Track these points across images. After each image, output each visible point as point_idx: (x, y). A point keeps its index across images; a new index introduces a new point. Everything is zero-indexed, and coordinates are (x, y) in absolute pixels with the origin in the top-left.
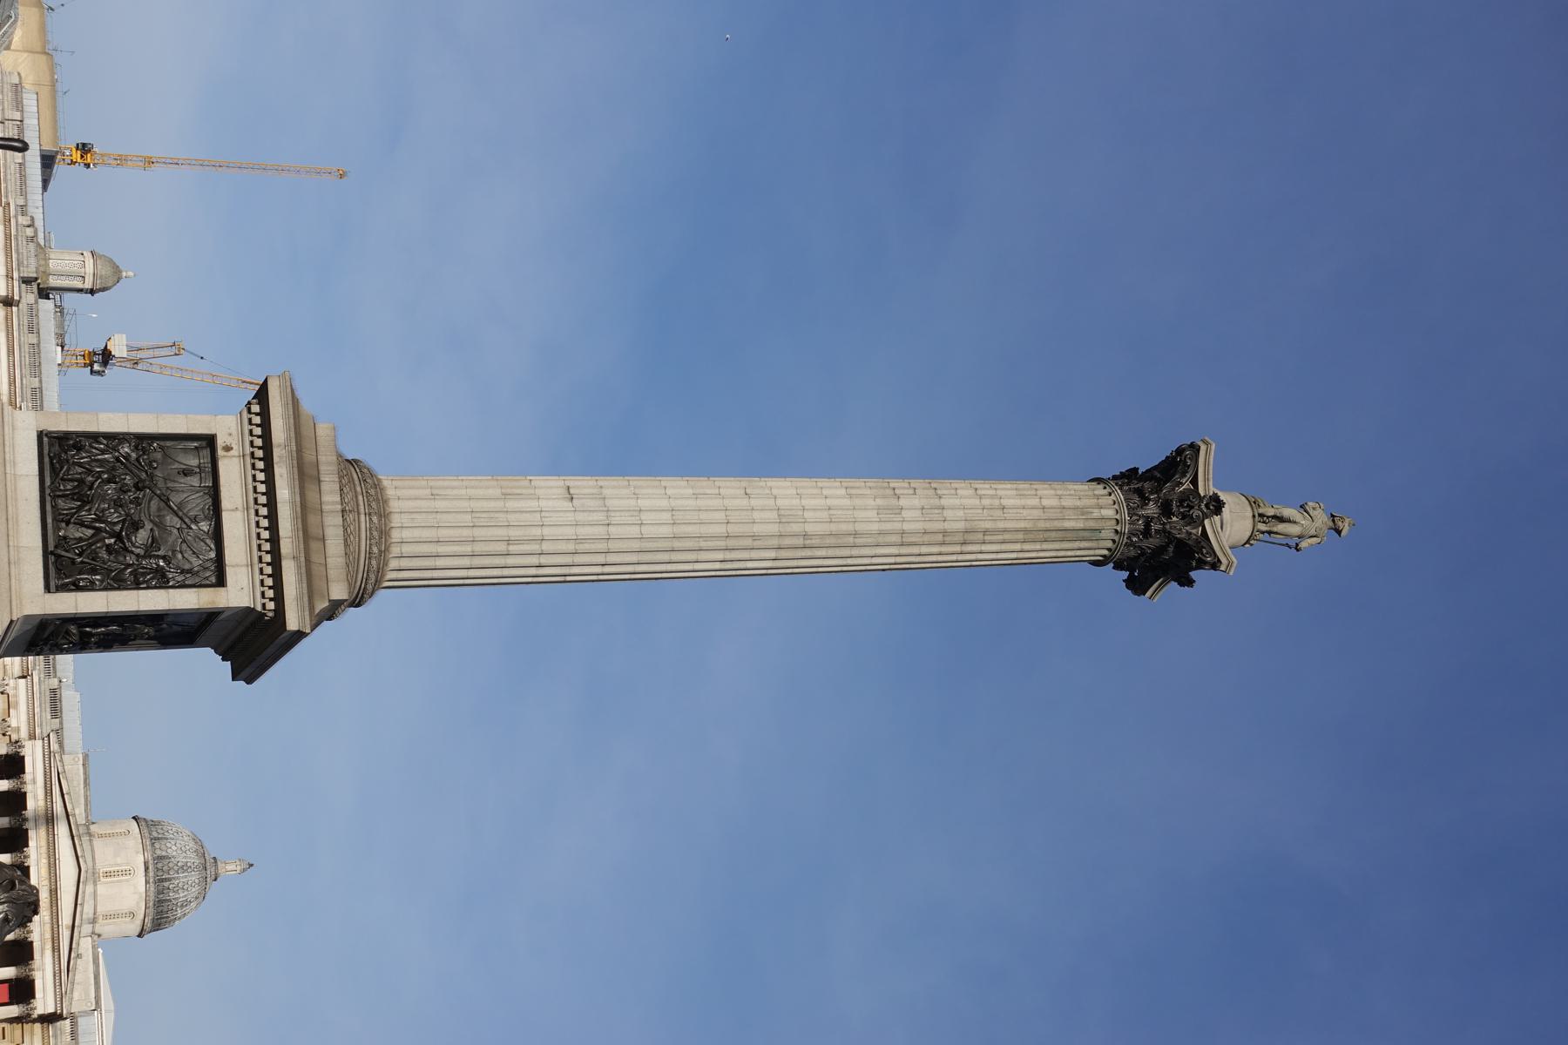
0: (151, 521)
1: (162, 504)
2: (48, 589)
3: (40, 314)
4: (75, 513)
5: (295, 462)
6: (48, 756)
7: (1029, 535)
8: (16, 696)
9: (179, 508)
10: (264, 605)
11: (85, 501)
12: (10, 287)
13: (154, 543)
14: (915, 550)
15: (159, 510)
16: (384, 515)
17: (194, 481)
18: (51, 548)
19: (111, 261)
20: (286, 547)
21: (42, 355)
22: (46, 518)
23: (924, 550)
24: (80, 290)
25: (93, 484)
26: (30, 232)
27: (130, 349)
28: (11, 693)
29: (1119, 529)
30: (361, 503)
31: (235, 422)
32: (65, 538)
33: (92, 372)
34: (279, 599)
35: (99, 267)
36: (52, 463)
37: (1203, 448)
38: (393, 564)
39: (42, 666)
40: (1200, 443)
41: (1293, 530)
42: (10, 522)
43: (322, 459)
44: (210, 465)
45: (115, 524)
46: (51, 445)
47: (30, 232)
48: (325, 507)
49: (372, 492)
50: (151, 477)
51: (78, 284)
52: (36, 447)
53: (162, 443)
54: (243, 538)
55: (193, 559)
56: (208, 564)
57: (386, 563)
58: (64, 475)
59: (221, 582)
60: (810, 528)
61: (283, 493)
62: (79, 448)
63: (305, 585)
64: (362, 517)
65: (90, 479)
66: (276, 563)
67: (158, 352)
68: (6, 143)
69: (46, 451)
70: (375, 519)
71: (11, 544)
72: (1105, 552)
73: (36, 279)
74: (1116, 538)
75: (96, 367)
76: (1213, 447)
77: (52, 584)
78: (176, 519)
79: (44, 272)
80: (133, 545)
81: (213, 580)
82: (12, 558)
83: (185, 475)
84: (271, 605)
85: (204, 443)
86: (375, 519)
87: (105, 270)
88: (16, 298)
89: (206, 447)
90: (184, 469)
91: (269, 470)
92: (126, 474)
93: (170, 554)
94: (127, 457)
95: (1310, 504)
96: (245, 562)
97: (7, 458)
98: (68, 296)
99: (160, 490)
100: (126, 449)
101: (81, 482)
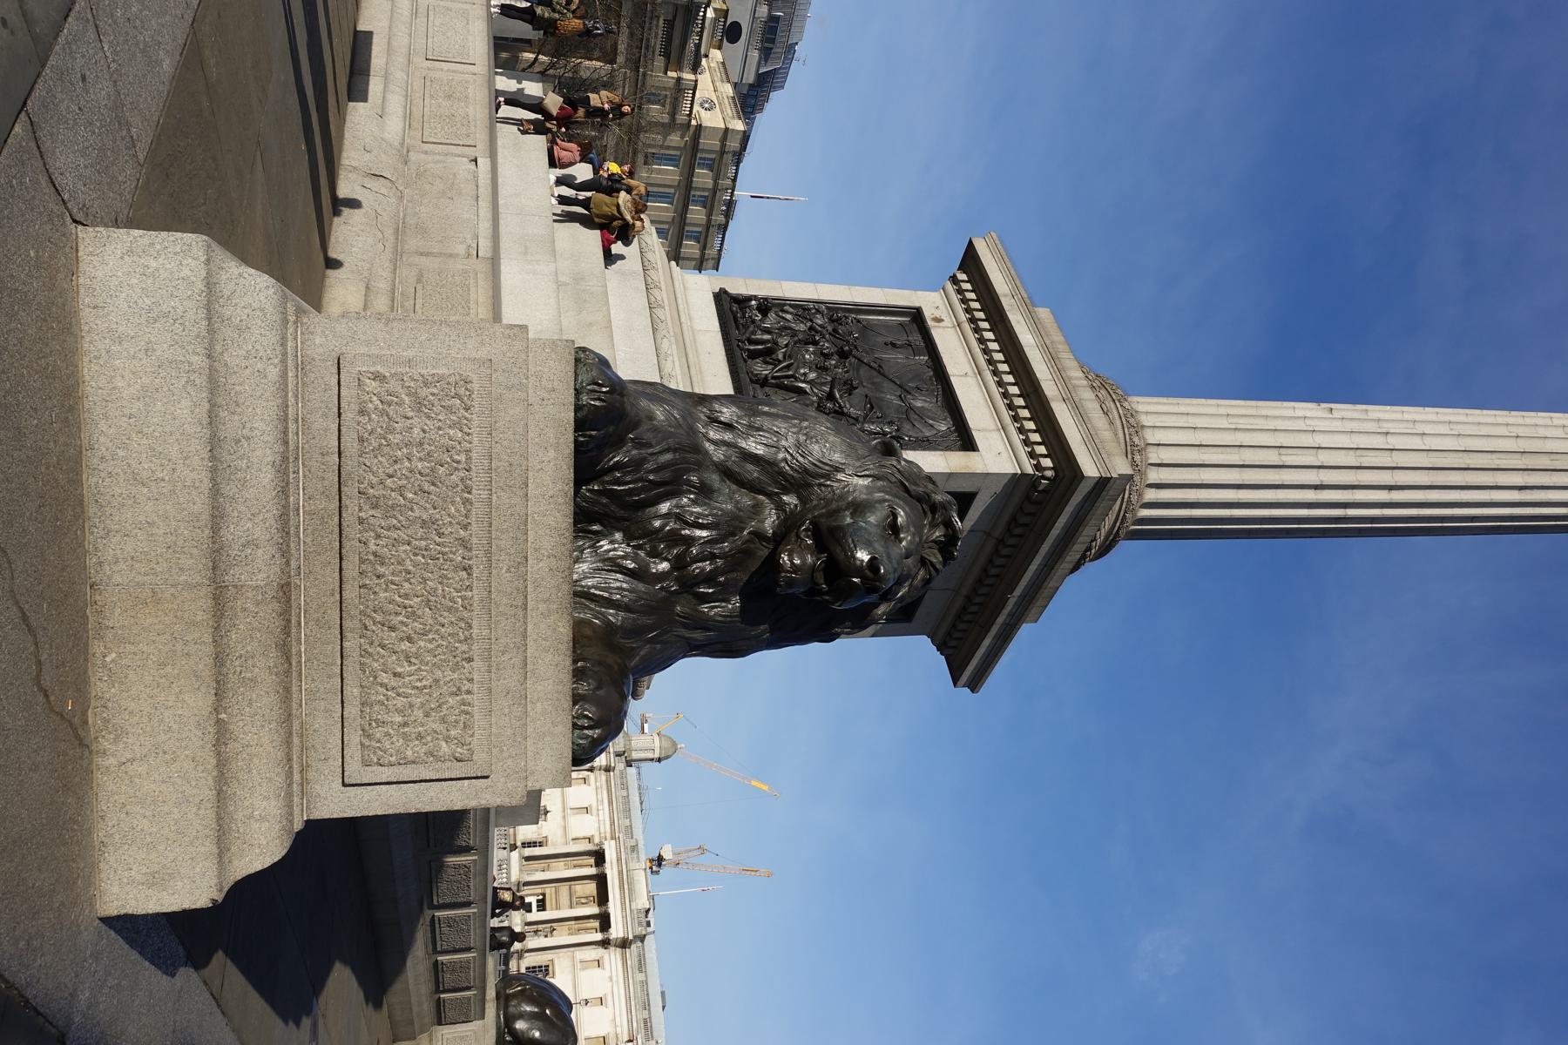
3: (628, 777)
10: (1038, 467)
19: (670, 738)
24: (653, 760)
27: (674, 854)
39: (643, 1034)
42: (692, 369)
51: (650, 755)
54: (982, 402)
67: (690, 854)
73: (624, 752)
75: (655, 868)
87: (666, 744)
88: (613, 765)
98: (643, 764)
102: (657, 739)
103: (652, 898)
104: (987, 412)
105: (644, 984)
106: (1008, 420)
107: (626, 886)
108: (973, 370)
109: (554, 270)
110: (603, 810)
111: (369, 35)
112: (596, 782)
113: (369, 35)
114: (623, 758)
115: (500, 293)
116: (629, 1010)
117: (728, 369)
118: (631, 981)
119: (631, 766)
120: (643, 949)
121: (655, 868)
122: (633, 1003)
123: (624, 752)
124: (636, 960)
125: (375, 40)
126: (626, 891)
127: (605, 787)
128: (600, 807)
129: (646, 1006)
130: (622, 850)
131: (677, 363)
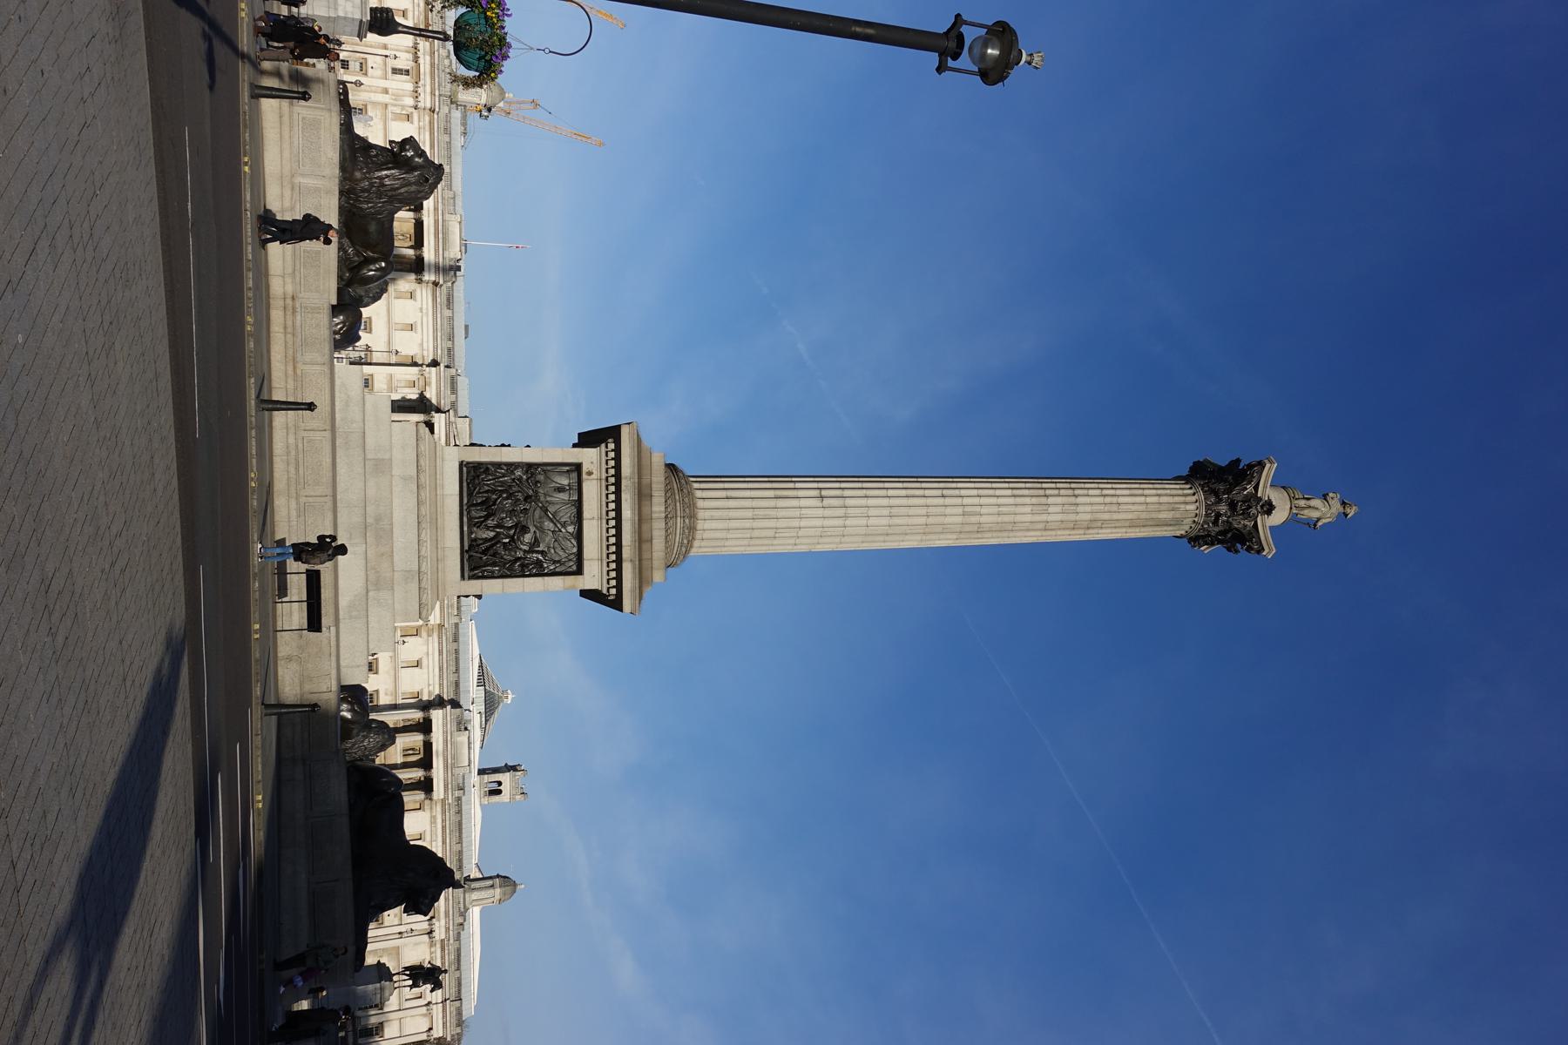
0: (535, 526)
1: (543, 513)
5: (636, 491)
6: (449, 424)
7: (1133, 524)
8: (429, 378)
9: (554, 516)
13: (536, 542)
14: (1053, 533)
15: (540, 518)
16: (693, 517)
17: (564, 496)
18: (466, 548)
20: (626, 553)
23: (1059, 532)
25: (496, 500)
28: (427, 376)
29: (1196, 520)
30: (678, 508)
32: (475, 540)
34: (619, 587)
36: (468, 484)
37: (1268, 466)
38: (696, 543)
40: (1266, 461)
41: (1315, 514)
43: (654, 479)
45: (510, 528)
46: (468, 472)
48: (654, 516)
49: (686, 500)
50: (536, 493)
53: (545, 468)
55: (561, 553)
56: (573, 556)
57: (691, 547)
58: (477, 493)
59: (579, 571)
60: (983, 519)
61: (627, 513)
63: (637, 581)
64: (679, 519)
65: (494, 497)
66: (619, 561)
69: (465, 478)
70: (687, 521)
71: (439, 546)
72: (1183, 532)
74: (1193, 526)
76: (1276, 465)
78: (552, 525)
80: (522, 544)
81: (574, 568)
82: (439, 557)
83: (560, 492)
84: (613, 591)
86: (687, 521)
88: (437, 110)
90: (558, 488)
91: (618, 493)
92: (519, 492)
93: (546, 549)
94: (520, 479)
95: (1331, 495)
96: (596, 557)
100: (518, 473)
101: (488, 499)
103: (465, 247)
104: (597, 547)
105: (451, 319)
106: (605, 556)
107: (441, 236)
112: (419, 121)
116: (435, 339)
118: (439, 315)
120: (453, 290)
122: (439, 334)
124: (445, 299)
126: (441, 241)
127: (427, 128)
129: (451, 337)
130: (440, 201)
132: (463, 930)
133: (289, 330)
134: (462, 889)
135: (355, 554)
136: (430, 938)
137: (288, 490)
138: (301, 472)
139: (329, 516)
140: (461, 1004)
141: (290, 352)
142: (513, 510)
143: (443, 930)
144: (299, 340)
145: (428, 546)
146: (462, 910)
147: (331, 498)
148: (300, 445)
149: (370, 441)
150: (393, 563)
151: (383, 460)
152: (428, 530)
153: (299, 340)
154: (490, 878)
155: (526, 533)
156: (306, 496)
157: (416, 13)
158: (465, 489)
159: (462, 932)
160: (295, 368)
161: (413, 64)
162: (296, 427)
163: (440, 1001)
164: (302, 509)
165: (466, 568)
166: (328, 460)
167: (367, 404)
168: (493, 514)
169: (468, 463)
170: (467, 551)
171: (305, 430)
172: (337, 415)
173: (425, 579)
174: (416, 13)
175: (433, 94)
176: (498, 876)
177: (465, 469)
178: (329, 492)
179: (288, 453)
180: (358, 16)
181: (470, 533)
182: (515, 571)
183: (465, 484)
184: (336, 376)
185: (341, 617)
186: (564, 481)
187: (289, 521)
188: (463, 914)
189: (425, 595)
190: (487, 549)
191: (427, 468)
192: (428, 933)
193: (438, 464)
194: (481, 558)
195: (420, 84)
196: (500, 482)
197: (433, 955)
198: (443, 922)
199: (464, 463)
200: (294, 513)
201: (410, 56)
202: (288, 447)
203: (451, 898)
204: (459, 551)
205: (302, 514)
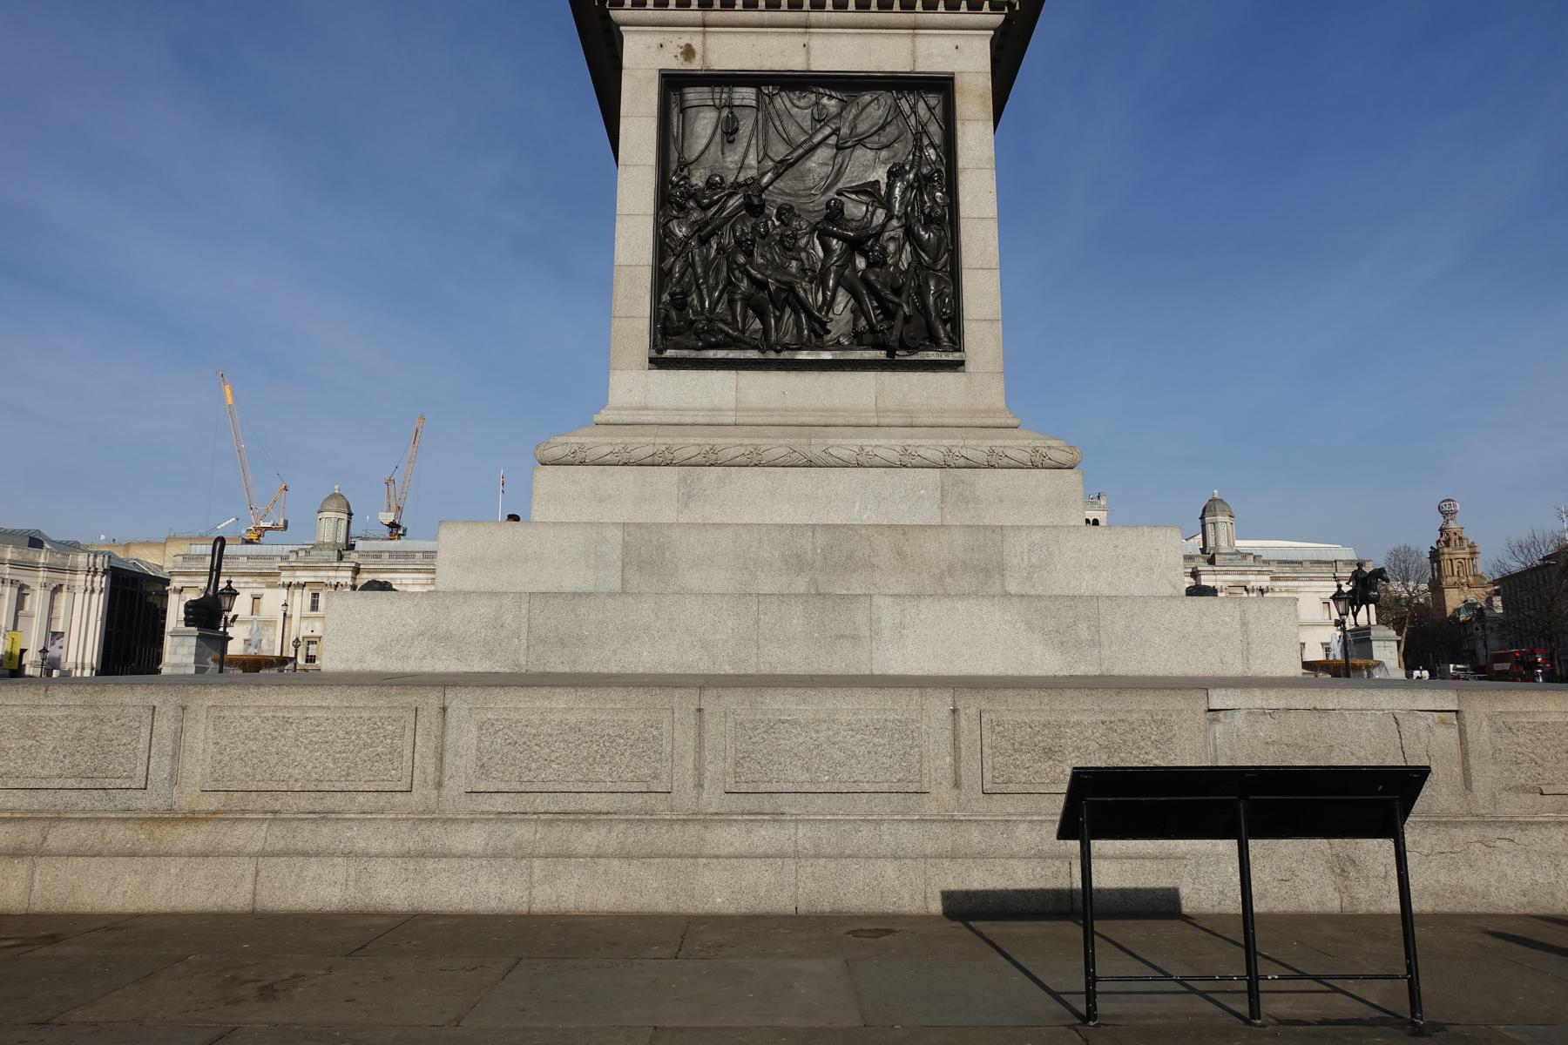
2: (957, 366)
4: (809, 315)
11: (789, 297)
12: (345, 569)
18: (881, 355)
19: (326, 500)
21: (398, 550)
22: (824, 361)
24: (349, 523)
26: (302, 554)
31: (637, 37)
33: (403, 535)
35: (331, 508)
42: (833, 420)
44: (717, 89)
46: (678, 346)
47: (302, 554)
50: (736, 187)
51: (344, 524)
52: (682, 372)
53: (674, 166)
54: (858, 41)
59: (943, 86)
62: (680, 303)
65: (744, 285)
67: (392, 494)
68: (217, 553)
69: (693, 354)
71: (874, 421)
73: (339, 551)
75: (401, 532)
77: (956, 356)
79: (334, 545)
81: (933, 100)
82: (901, 421)
83: (736, 130)
85: (674, 98)
87: (334, 504)
88: (354, 565)
89: (682, 95)
90: (726, 133)
92: (733, 229)
96: (907, 41)
97: (707, 420)
98: (352, 532)
99: (764, 174)
100: (681, 232)
101: (748, 302)
102: (326, 514)
108: (799, 33)
109: (889, 600)
110: (401, 579)
111: (947, 896)
113: (947, 896)
114: (344, 553)
115: (959, 677)
117: (816, 373)
119: (354, 545)
121: (401, 532)
123: (339, 551)
125: (954, 885)
128: (399, 582)
131: (883, 442)
132: (1261, 556)
133: (30, 835)
134: (1216, 556)
135: (902, 626)
136: (1267, 592)
137: (668, 856)
138: (603, 803)
139: (779, 703)
140: (1341, 561)
141: (120, 835)
142: (781, 242)
143: (1260, 577)
144: (85, 801)
145: (876, 442)
146: (1239, 557)
147: (710, 694)
148: (499, 803)
149: (572, 581)
150: (923, 528)
151: (625, 545)
152: (831, 441)
153: (85, 801)
154: (1204, 526)
155: (842, 211)
156: (699, 785)
157: (255, 585)
158: (721, 354)
159: (1264, 558)
160: (191, 818)
161: (306, 589)
162: (429, 817)
163: (1335, 584)
164: (750, 803)
165: (932, 356)
166: (560, 701)
167: (467, 583)
168: (791, 289)
169: (654, 345)
170: (891, 353)
171: (439, 785)
172: (478, 668)
173: (964, 452)
174: (255, 585)
175: (337, 569)
176: (1202, 518)
177: (669, 353)
178: (685, 702)
179: (522, 854)
180: (194, 641)
181: (838, 346)
182: (940, 240)
183: (711, 354)
184: (356, 667)
185: (1093, 670)
186: (704, 124)
187: (796, 855)
188: (1245, 556)
189: (1009, 452)
190: (882, 303)
191: (659, 441)
192: (1262, 594)
193: (652, 419)
194: (907, 319)
195: (325, 580)
196: (706, 271)
197: (1283, 590)
198: (1251, 577)
199: (654, 354)
200: (765, 836)
201: (298, 592)
202: (498, 855)
203: (1225, 569)
204: (888, 377)
205: (768, 804)
